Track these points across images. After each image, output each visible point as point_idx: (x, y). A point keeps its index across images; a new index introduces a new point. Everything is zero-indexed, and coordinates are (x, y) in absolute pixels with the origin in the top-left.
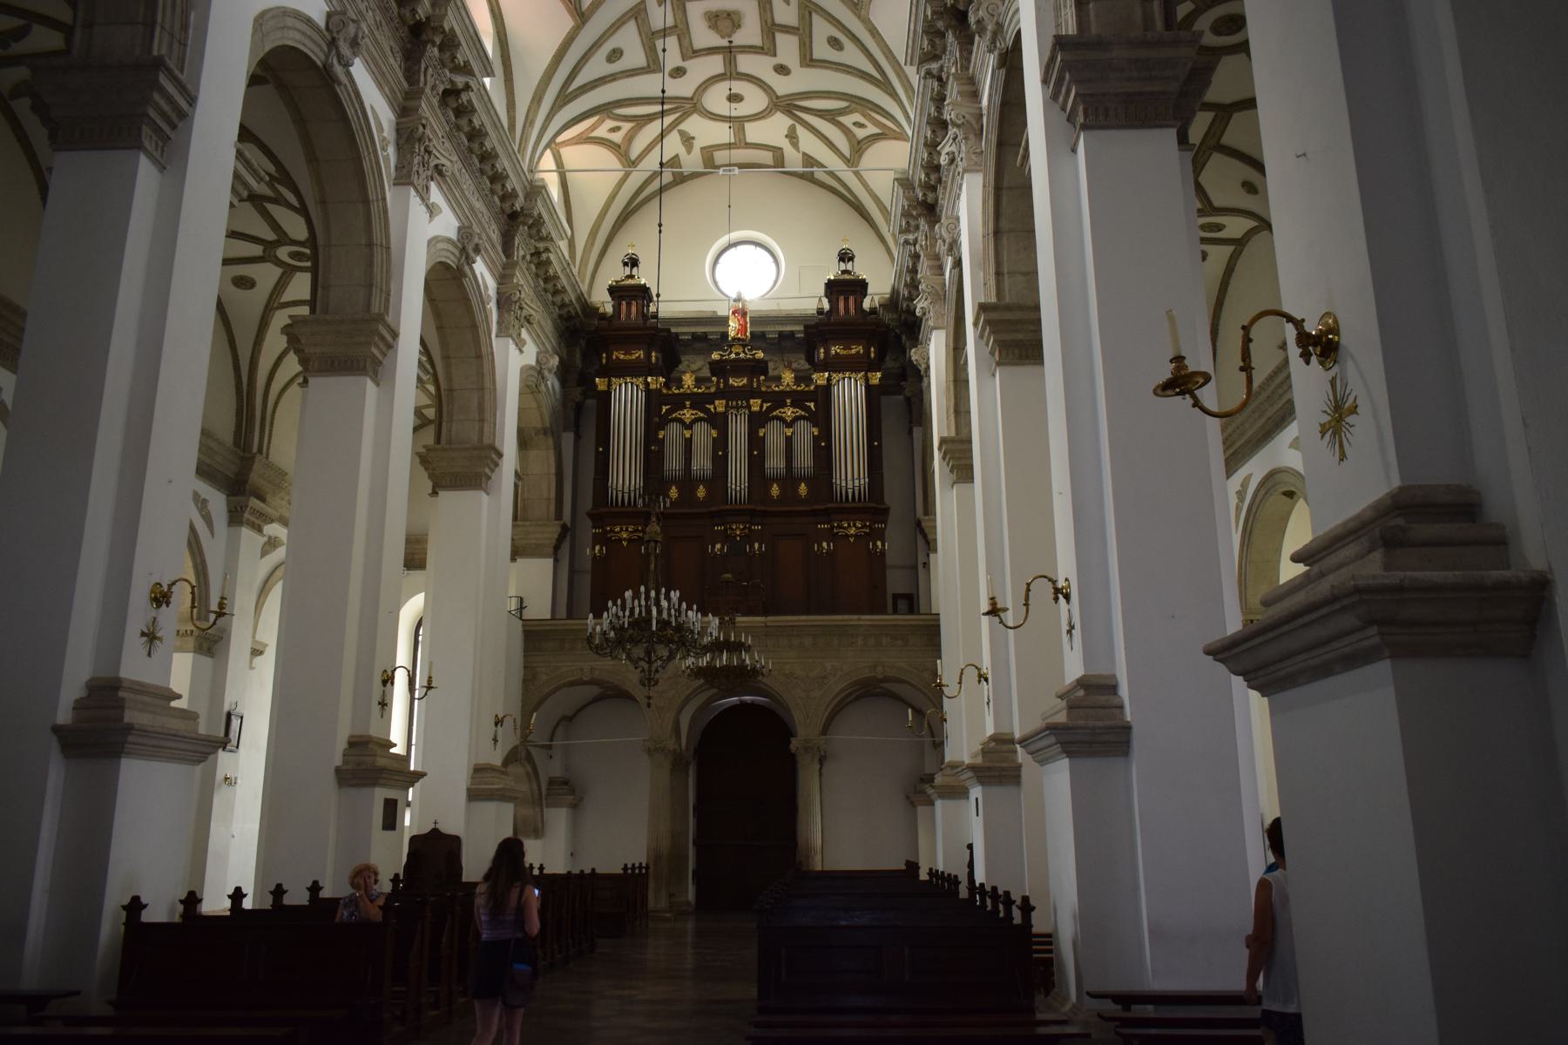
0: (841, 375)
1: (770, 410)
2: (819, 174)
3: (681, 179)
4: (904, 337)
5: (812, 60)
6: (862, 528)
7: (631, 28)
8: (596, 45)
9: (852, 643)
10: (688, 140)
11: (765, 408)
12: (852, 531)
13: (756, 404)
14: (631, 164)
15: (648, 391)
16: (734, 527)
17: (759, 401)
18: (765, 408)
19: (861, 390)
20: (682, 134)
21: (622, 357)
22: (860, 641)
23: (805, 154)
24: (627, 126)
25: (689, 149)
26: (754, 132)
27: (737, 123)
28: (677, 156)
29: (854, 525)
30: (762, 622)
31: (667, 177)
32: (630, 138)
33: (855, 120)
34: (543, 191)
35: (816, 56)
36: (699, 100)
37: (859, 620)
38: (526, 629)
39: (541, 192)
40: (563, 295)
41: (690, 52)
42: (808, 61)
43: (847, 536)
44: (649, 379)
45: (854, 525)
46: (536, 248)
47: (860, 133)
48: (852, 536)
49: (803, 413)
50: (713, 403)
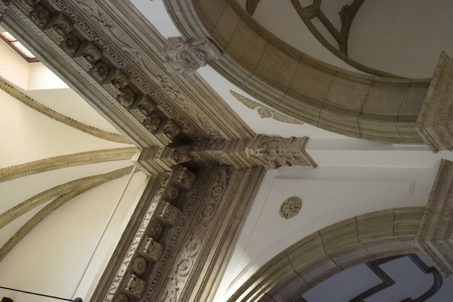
4: (197, 155)
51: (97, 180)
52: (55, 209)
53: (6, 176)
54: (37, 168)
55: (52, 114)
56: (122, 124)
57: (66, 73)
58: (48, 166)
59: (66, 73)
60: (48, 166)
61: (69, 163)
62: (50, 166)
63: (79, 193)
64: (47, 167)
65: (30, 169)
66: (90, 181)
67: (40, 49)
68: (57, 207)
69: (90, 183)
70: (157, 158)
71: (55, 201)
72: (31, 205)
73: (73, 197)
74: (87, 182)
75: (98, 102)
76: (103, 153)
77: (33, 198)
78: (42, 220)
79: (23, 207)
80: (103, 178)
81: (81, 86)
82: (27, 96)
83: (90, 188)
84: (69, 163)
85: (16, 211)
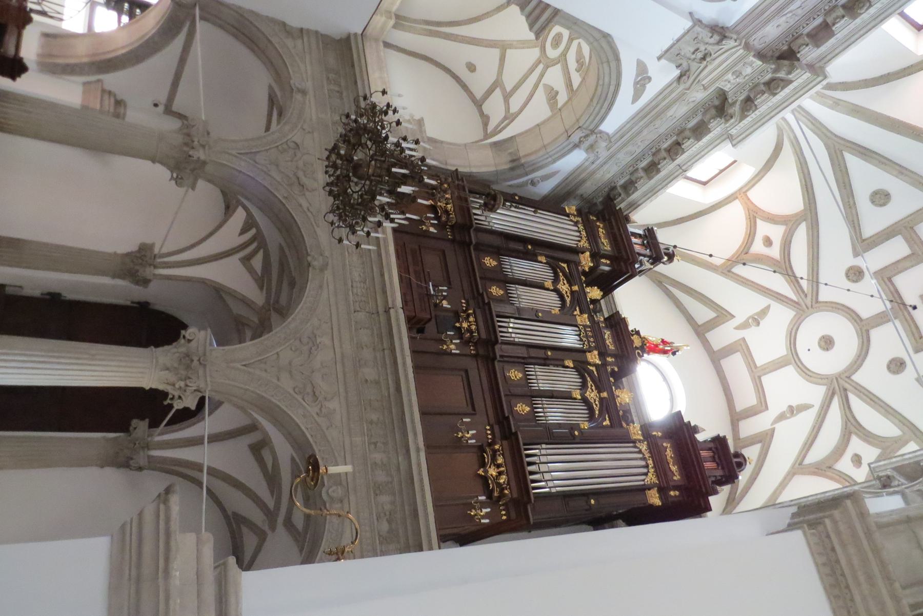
0: (647, 455)
1: (591, 374)
6: (499, 485)
9: (375, 444)
10: (756, 320)
11: (591, 368)
12: (493, 472)
13: (593, 357)
15: (576, 251)
16: (471, 319)
17: (598, 362)
18: (591, 368)
19: (636, 482)
20: (764, 312)
21: (601, 230)
22: (378, 457)
23: (773, 431)
25: (744, 326)
27: (793, 358)
28: (733, 316)
29: (500, 473)
30: (394, 301)
32: (760, 259)
34: (820, 78)
37: (418, 450)
38: (352, 38)
39: (818, 76)
40: (645, 177)
43: (483, 464)
44: (588, 254)
45: (500, 473)
46: (734, 103)
48: (486, 472)
49: (597, 412)
50: (582, 312)
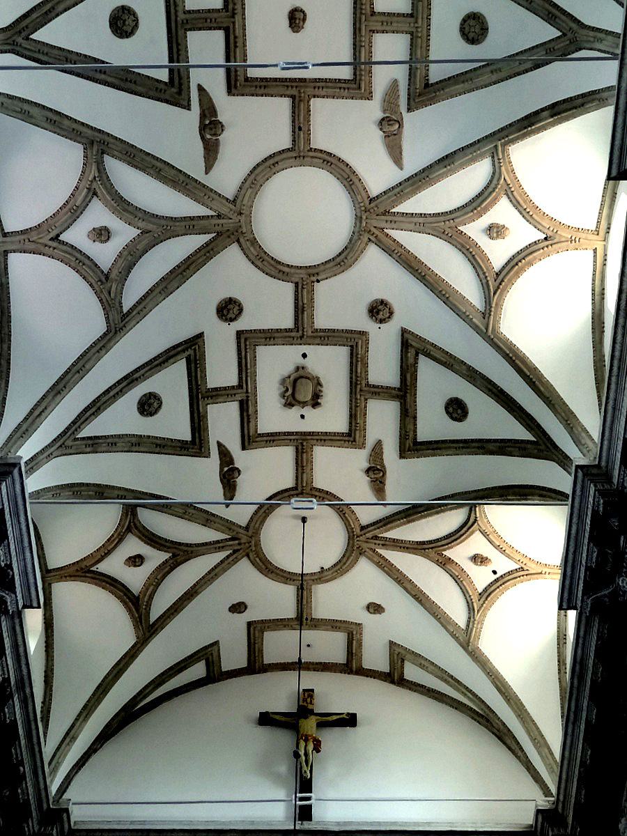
2: (412, 672)
3: (215, 675)
5: (415, 443)
7: (178, 370)
8: (130, 380)
14: (147, 630)
24: (156, 558)
26: (328, 599)
31: (198, 671)
33: (472, 554)
34: (16, 472)
35: (424, 433)
36: (257, 533)
39: (11, 473)
41: (250, 439)
42: (411, 446)
47: (481, 577)
51: (520, 753)
52: (473, 718)
53: (474, 655)
54: (498, 684)
55: (562, 672)
56: (564, 776)
57: (574, 696)
58: (506, 694)
59: (574, 696)
60: (506, 694)
61: (520, 716)
62: (506, 697)
63: (500, 738)
64: (504, 694)
65: (493, 677)
66: (516, 746)
67: (578, 659)
68: (475, 720)
69: (514, 746)
70: (553, 831)
71: (480, 714)
72: (463, 692)
73: (493, 733)
74: (513, 742)
75: (568, 742)
76: (547, 751)
77: (470, 691)
78: (456, 709)
79: (456, 684)
80: (524, 759)
81: (572, 718)
82: (565, 635)
83: (510, 749)
84: (520, 716)
85: (450, 680)
